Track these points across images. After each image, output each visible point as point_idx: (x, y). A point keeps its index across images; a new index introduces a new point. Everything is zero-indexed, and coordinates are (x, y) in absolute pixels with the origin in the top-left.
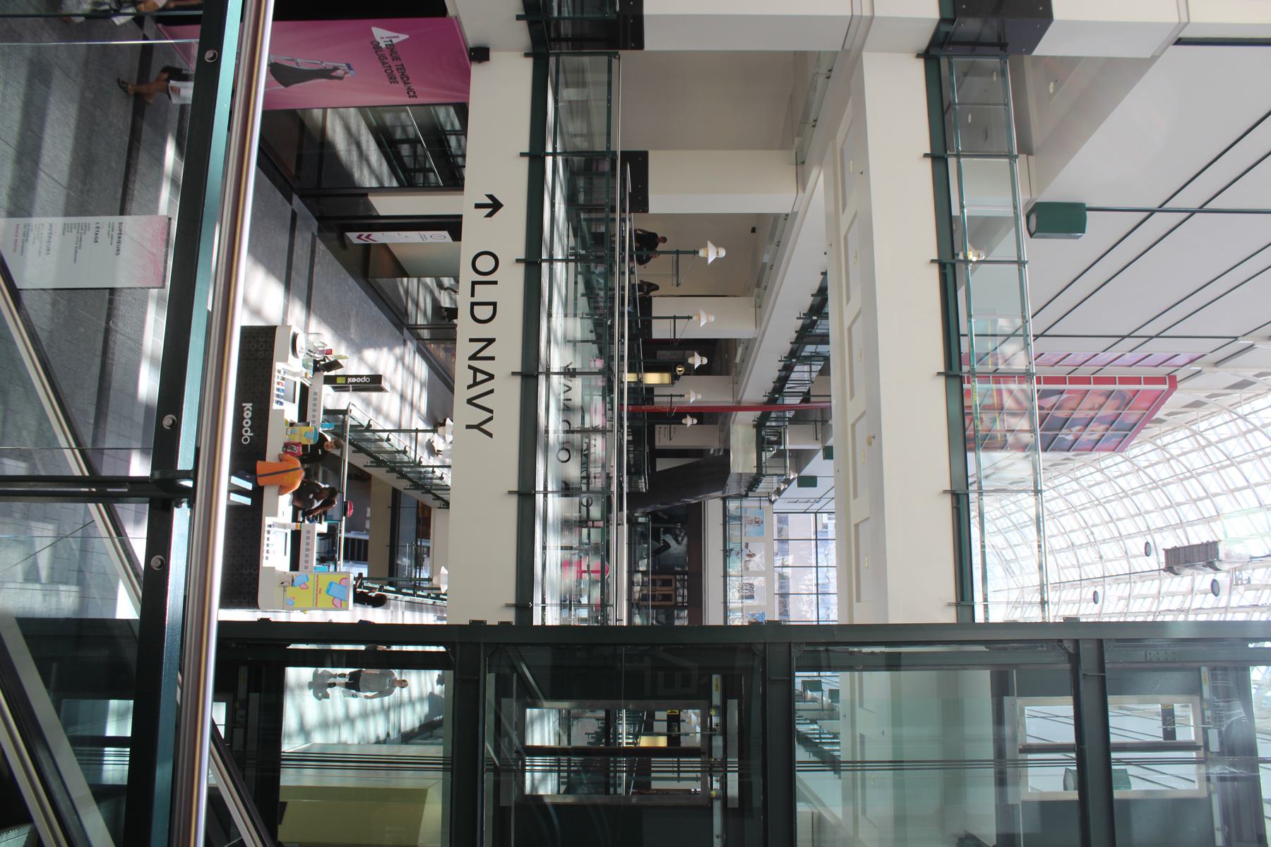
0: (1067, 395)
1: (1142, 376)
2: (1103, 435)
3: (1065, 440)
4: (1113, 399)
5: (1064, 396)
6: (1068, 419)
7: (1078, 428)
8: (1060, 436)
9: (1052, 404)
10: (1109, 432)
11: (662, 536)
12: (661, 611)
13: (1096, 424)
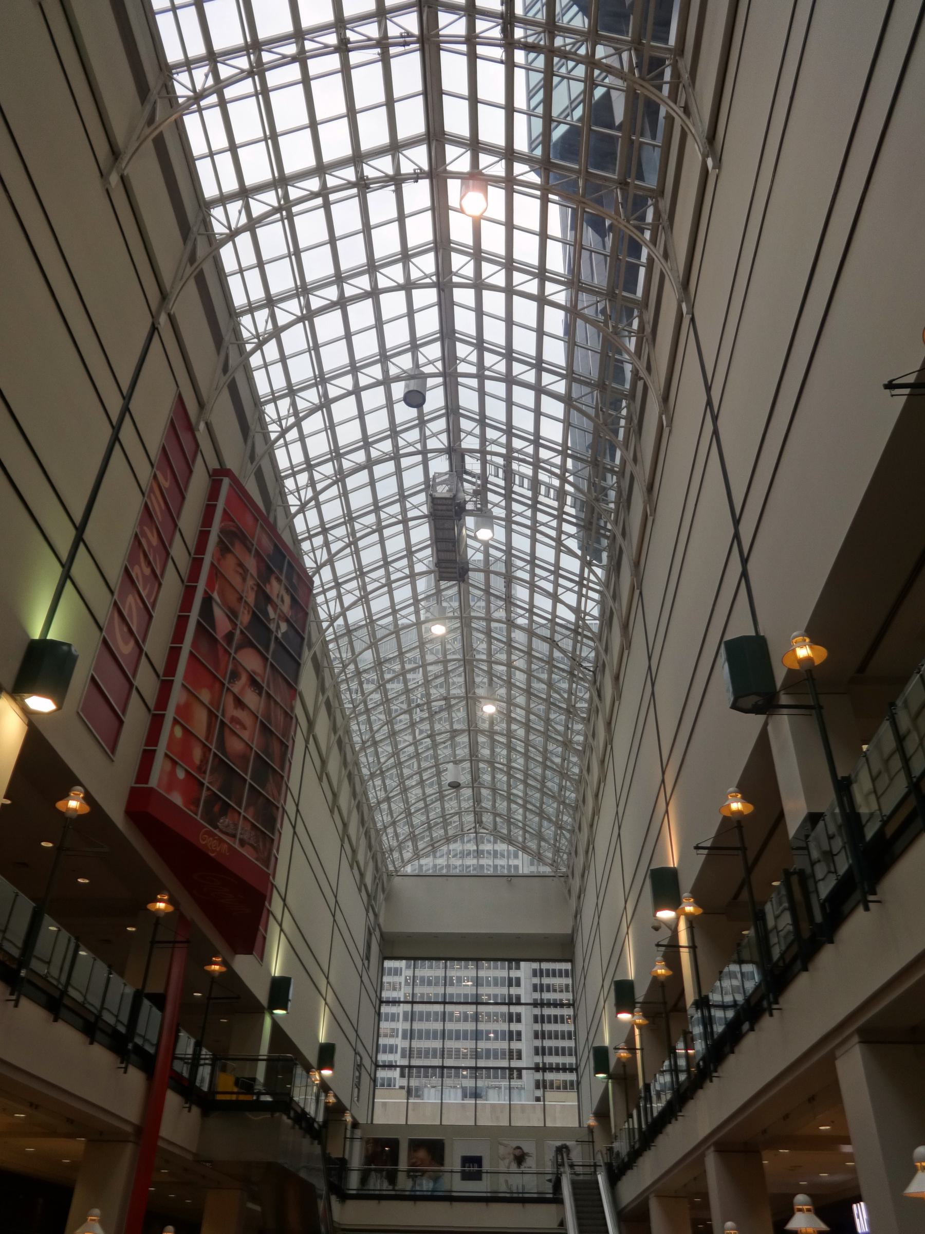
1: (206, 502)
2: (287, 589)
4: (233, 545)
5: (215, 596)
6: (254, 612)
7: (270, 610)
8: (279, 636)
9: (227, 620)
10: (283, 578)
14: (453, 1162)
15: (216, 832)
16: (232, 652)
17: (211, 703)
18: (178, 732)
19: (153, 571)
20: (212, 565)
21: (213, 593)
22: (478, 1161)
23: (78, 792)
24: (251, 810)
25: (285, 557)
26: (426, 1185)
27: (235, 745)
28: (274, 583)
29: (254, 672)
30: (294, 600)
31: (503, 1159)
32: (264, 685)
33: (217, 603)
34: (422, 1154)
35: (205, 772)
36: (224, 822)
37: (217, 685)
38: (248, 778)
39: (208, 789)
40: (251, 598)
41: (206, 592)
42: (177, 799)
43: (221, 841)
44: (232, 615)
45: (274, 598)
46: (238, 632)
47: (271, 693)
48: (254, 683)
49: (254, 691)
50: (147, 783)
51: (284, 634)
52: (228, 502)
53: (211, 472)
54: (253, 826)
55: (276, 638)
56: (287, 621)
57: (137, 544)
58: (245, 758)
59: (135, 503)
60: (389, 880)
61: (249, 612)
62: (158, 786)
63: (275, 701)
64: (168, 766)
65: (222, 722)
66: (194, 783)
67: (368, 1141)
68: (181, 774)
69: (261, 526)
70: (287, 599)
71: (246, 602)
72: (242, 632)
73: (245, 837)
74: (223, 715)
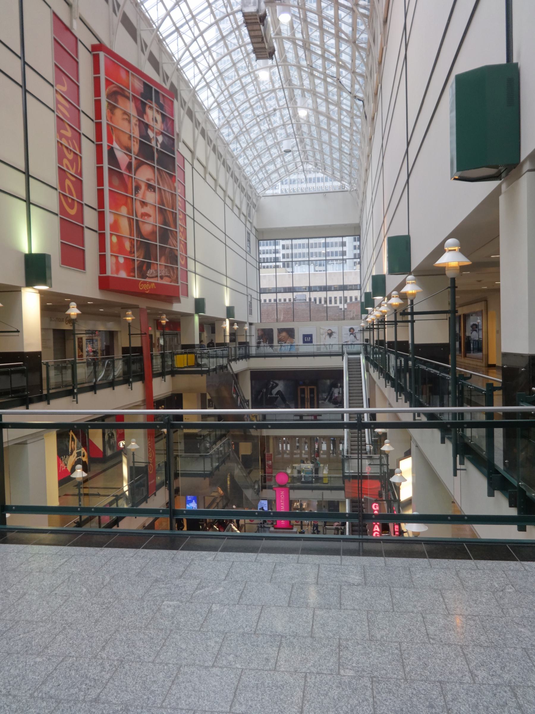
0: (114, 143)
2: (157, 111)
3: (163, 143)
4: (116, 102)
5: (115, 145)
6: (140, 141)
7: (150, 133)
8: (159, 147)
9: (125, 156)
11: (274, 395)
12: (320, 396)
13: (145, 117)
14: (298, 339)
15: (147, 280)
16: (133, 176)
17: (128, 213)
18: (115, 239)
19: (75, 153)
20: (108, 124)
21: (112, 144)
22: (311, 336)
23: (73, 305)
24: (163, 258)
25: (152, 88)
26: (286, 349)
27: (146, 229)
28: (148, 111)
29: (148, 180)
30: (163, 116)
31: (323, 335)
32: (156, 185)
33: (117, 149)
34: (284, 334)
35: (134, 253)
36: (150, 273)
37: (129, 201)
38: (158, 244)
39: (138, 260)
40: (136, 133)
41: (108, 146)
42: (123, 274)
43: (150, 283)
44: (128, 149)
45: (151, 123)
46: (133, 159)
47: (161, 187)
48: (150, 187)
49: (151, 191)
50: (105, 273)
51: (163, 145)
52: (107, 74)
53: (90, 49)
54: (165, 266)
55: (157, 149)
56: (162, 133)
57: (60, 145)
58: (154, 233)
59: (51, 118)
60: (257, 200)
61: (137, 142)
62: (112, 273)
63: (164, 190)
64: (114, 259)
65: (137, 221)
66: (129, 264)
67: (258, 330)
68: (121, 260)
69: (132, 74)
70: (159, 118)
71: (134, 137)
72: (136, 158)
73: (163, 274)
74: (136, 216)
